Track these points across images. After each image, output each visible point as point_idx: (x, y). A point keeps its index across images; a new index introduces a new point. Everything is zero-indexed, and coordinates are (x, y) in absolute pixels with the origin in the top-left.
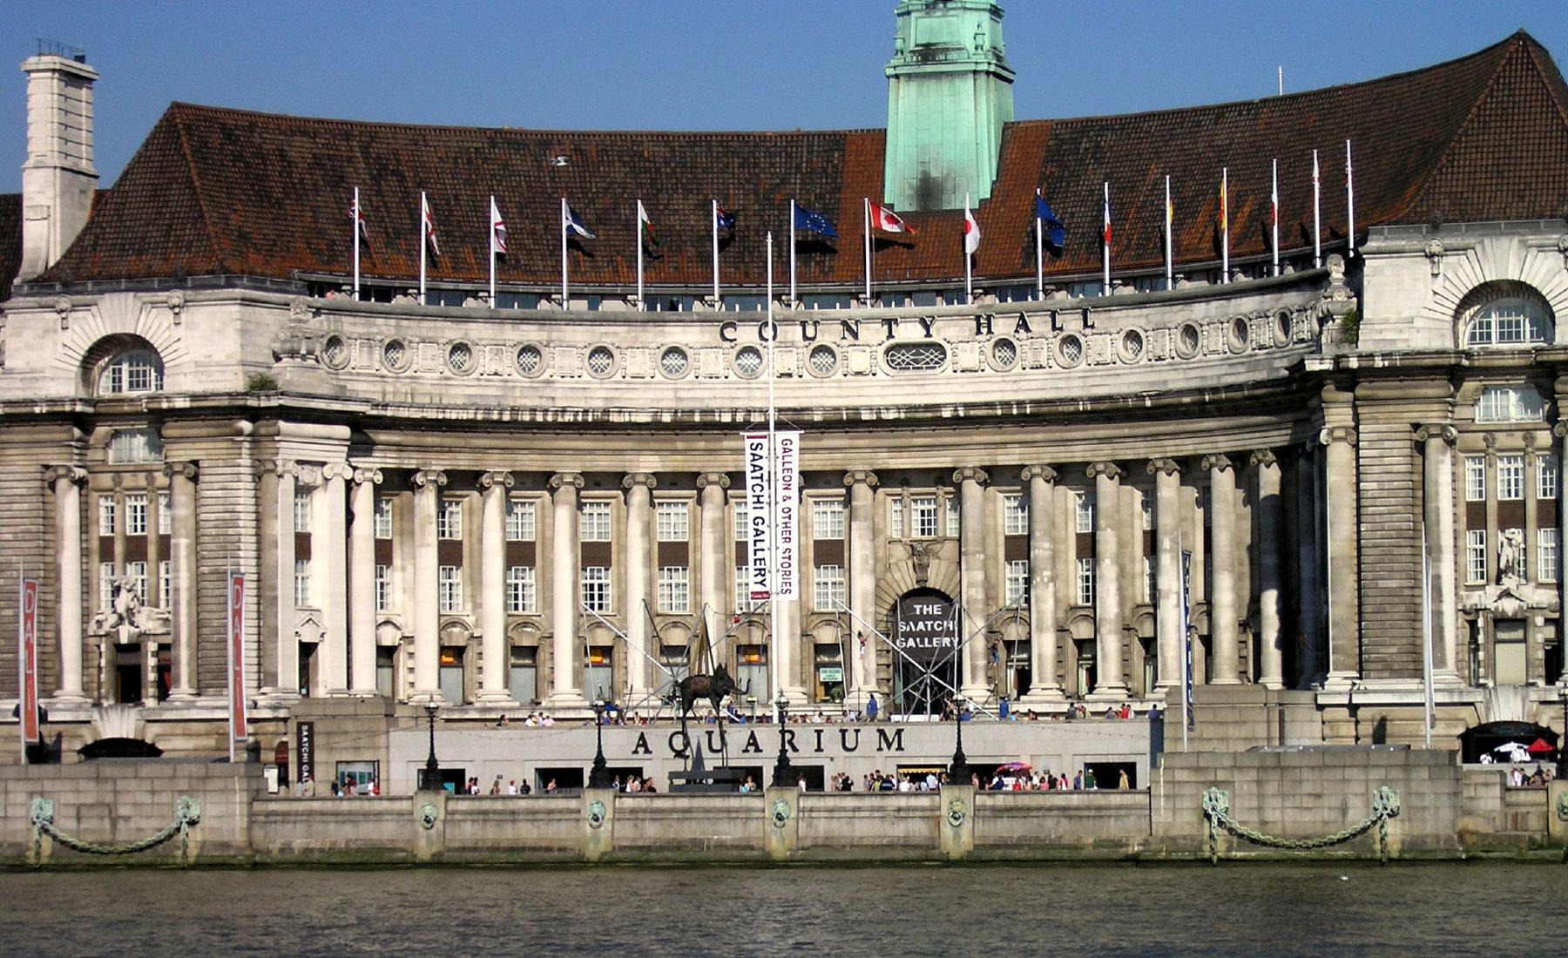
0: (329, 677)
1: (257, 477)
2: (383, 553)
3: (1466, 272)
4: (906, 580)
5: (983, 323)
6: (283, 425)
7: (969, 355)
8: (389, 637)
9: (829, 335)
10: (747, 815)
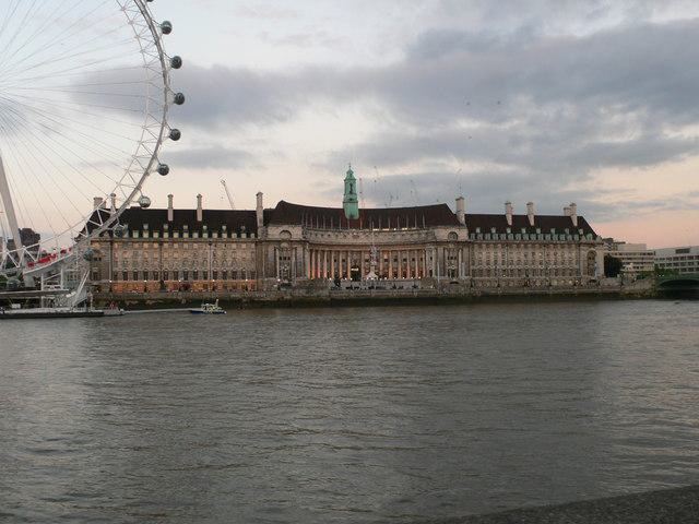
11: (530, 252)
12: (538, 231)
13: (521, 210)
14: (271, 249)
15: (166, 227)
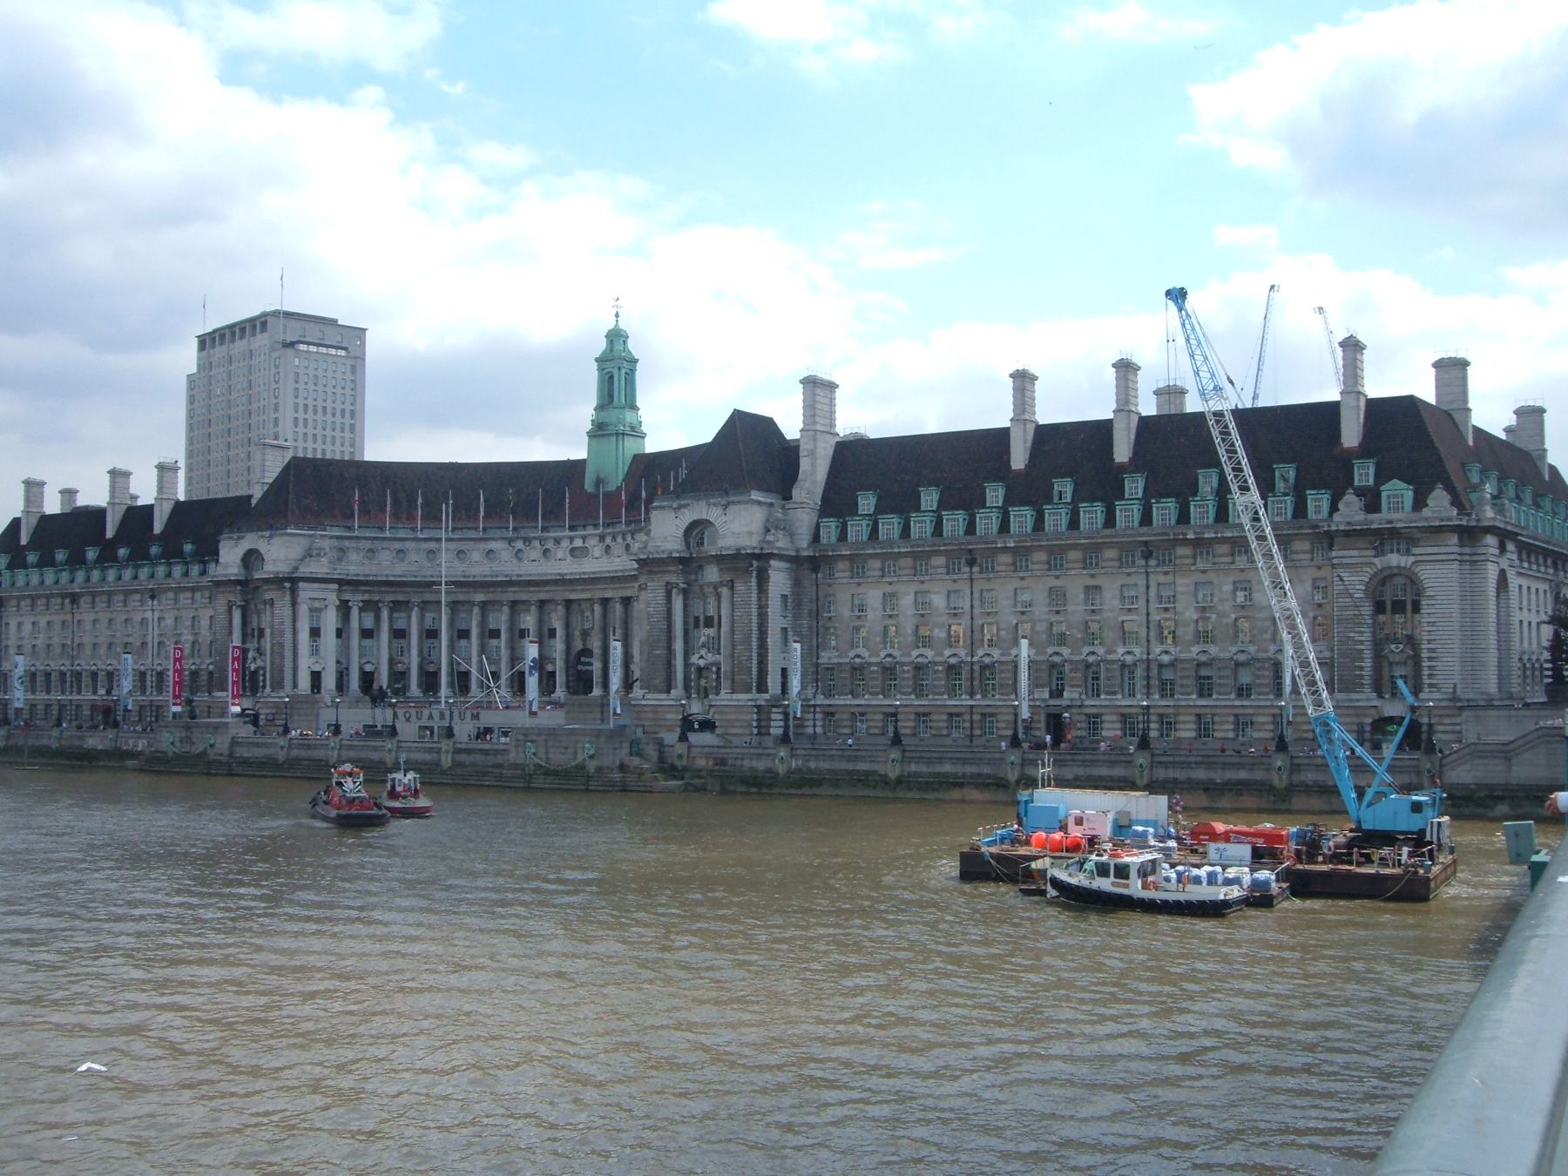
0: (329, 682)
1: (294, 604)
2: (367, 634)
3: (688, 516)
4: (578, 645)
5: (602, 538)
6: (301, 585)
7: (597, 551)
8: (368, 668)
9: (550, 545)
10: (382, 748)
11: (1074, 584)
12: (1135, 486)
13: (1075, 396)
14: (221, 603)
15: (91, 554)
